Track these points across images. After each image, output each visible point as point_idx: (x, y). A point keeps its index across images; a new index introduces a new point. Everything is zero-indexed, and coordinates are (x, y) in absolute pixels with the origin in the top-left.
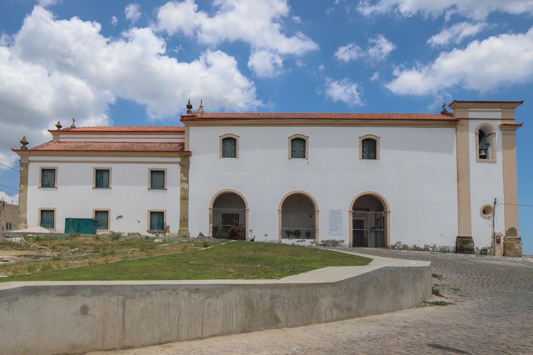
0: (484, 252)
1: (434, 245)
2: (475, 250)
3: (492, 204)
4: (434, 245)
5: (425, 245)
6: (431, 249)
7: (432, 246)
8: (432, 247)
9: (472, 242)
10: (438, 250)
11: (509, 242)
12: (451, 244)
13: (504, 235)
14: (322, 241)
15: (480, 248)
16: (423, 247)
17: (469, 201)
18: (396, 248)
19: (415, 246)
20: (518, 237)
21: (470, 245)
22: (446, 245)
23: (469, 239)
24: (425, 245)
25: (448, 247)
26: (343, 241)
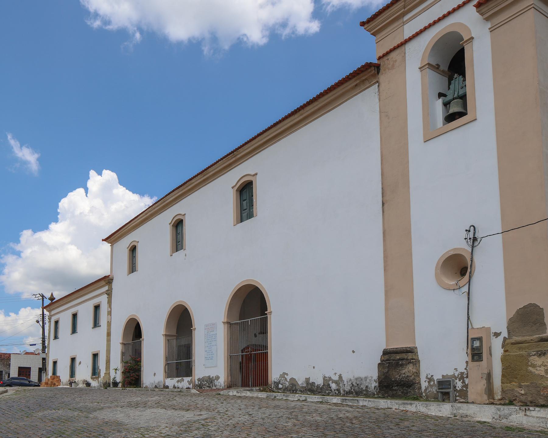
0: (445, 390)
1: (340, 377)
2: (424, 384)
3: (464, 246)
4: (340, 377)
5: (324, 378)
6: (334, 386)
7: (336, 378)
8: (336, 382)
10: (347, 388)
11: (515, 352)
14: (199, 380)
15: (438, 376)
16: (319, 382)
17: (409, 254)
18: (280, 386)
19: (307, 380)
22: (363, 376)
24: (324, 378)
25: (366, 378)
26: (218, 378)
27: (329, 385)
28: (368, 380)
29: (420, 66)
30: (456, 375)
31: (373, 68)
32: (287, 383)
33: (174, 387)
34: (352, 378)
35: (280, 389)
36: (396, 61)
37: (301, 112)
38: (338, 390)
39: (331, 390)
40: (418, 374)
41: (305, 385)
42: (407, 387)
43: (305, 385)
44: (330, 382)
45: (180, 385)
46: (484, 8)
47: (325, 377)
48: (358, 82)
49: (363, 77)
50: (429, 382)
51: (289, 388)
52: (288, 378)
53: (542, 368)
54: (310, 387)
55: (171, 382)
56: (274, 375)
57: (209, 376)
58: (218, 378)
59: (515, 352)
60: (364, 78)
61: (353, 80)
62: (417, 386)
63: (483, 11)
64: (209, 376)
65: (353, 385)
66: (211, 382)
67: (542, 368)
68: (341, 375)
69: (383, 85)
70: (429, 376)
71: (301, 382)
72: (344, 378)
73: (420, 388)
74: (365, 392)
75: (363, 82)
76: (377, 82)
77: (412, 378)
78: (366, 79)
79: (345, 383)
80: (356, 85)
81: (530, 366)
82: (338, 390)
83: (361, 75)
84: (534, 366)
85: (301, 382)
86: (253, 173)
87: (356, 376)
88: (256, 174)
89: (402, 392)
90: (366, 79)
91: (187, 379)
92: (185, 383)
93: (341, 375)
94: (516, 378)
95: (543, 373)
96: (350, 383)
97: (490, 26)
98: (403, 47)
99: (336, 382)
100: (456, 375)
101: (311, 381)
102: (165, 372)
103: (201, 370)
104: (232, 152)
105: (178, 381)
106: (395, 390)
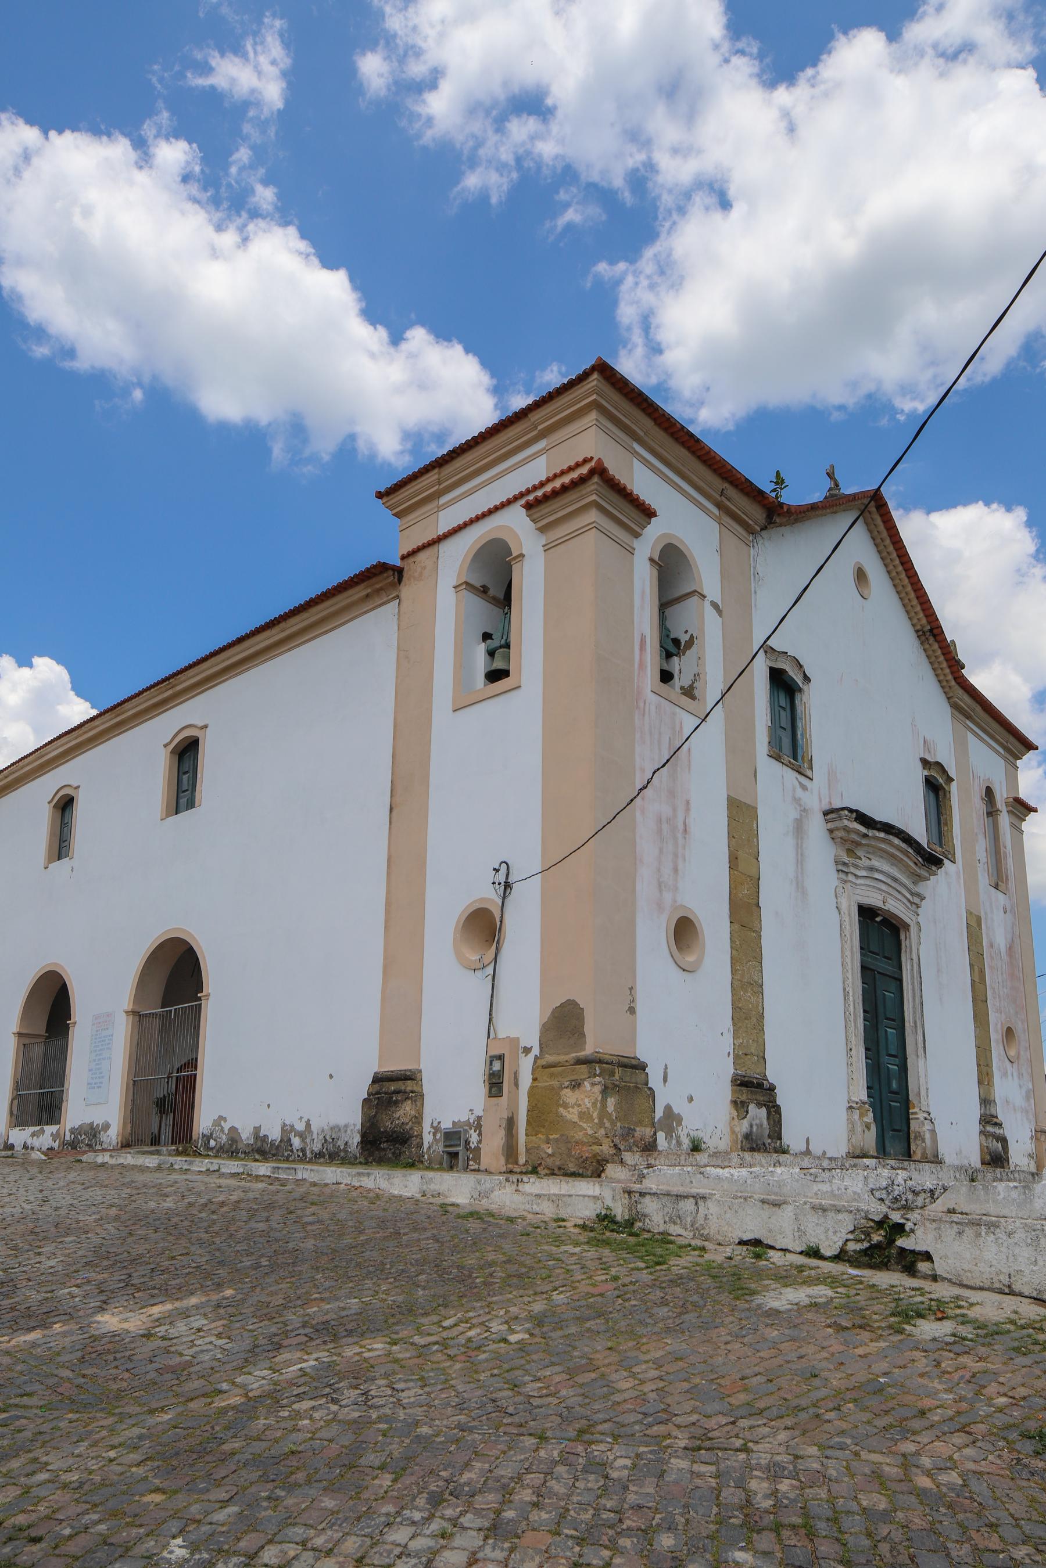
1: (308, 1124)
2: (427, 1138)
4: (308, 1124)
6: (296, 1142)
7: (300, 1127)
8: (301, 1135)
9: (418, 1097)
10: (317, 1147)
12: (342, 1112)
13: (536, 1051)
14: (73, 1131)
15: (447, 1125)
16: (274, 1134)
18: (212, 1143)
20: (588, 1050)
21: (407, 1109)
22: (342, 1122)
23: (400, 1085)
26: (106, 1126)
27: (290, 1140)
28: (349, 1131)
29: (455, 583)
30: (471, 1121)
31: (391, 572)
32: (224, 1137)
33: (25, 1147)
34: (326, 1128)
35: (212, 1149)
36: (424, 568)
37: (283, 625)
38: (303, 1150)
39: (292, 1151)
40: (418, 1119)
41: (252, 1141)
42: (401, 1144)
43: (252, 1141)
44: (292, 1135)
45: (36, 1142)
46: (538, 512)
47: (285, 1125)
48: (369, 590)
49: (377, 583)
50: (434, 1134)
51: (227, 1146)
52: (226, 1127)
53: (575, 1110)
54: (259, 1144)
55: (19, 1136)
56: (203, 1121)
57: (92, 1123)
58: (106, 1126)
59: (544, 1083)
60: (377, 586)
61: (362, 586)
62: (415, 1142)
63: (535, 516)
64: (92, 1123)
65: (326, 1140)
66: (95, 1136)
67: (575, 1110)
68: (309, 1120)
69: (404, 604)
70: (435, 1124)
71: (246, 1135)
72: (314, 1128)
73: (420, 1145)
74: (342, 1154)
75: (378, 591)
76: (398, 597)
77: (408, 1127)
78: (381, 589)
79: (315, 1136)
80: (367, 596)
81: (561, 1106)
82: (303, 1150)
83: (374, 580)
84: (566, 1106)
85: (246, 1135)
86: (200, 724)
87: (332, 1124)
88: (206, 727)
89: (393, 1153)
90: (381, 589)
91: (50, 1129)
92: (46, 1137)
93: (309, 1120)
94: (544, 1127)
95: (575, 1119)
96: (321, 1137)
97: (544, 543)
98: (435, 547)
99: (301, 1135)
100: (471, 1121)
101: (262, 1133)
102: (11, 1114)
103: (76, 1113)
104: (167, 679)
105: (33, 1135)
106: (384, 1149)
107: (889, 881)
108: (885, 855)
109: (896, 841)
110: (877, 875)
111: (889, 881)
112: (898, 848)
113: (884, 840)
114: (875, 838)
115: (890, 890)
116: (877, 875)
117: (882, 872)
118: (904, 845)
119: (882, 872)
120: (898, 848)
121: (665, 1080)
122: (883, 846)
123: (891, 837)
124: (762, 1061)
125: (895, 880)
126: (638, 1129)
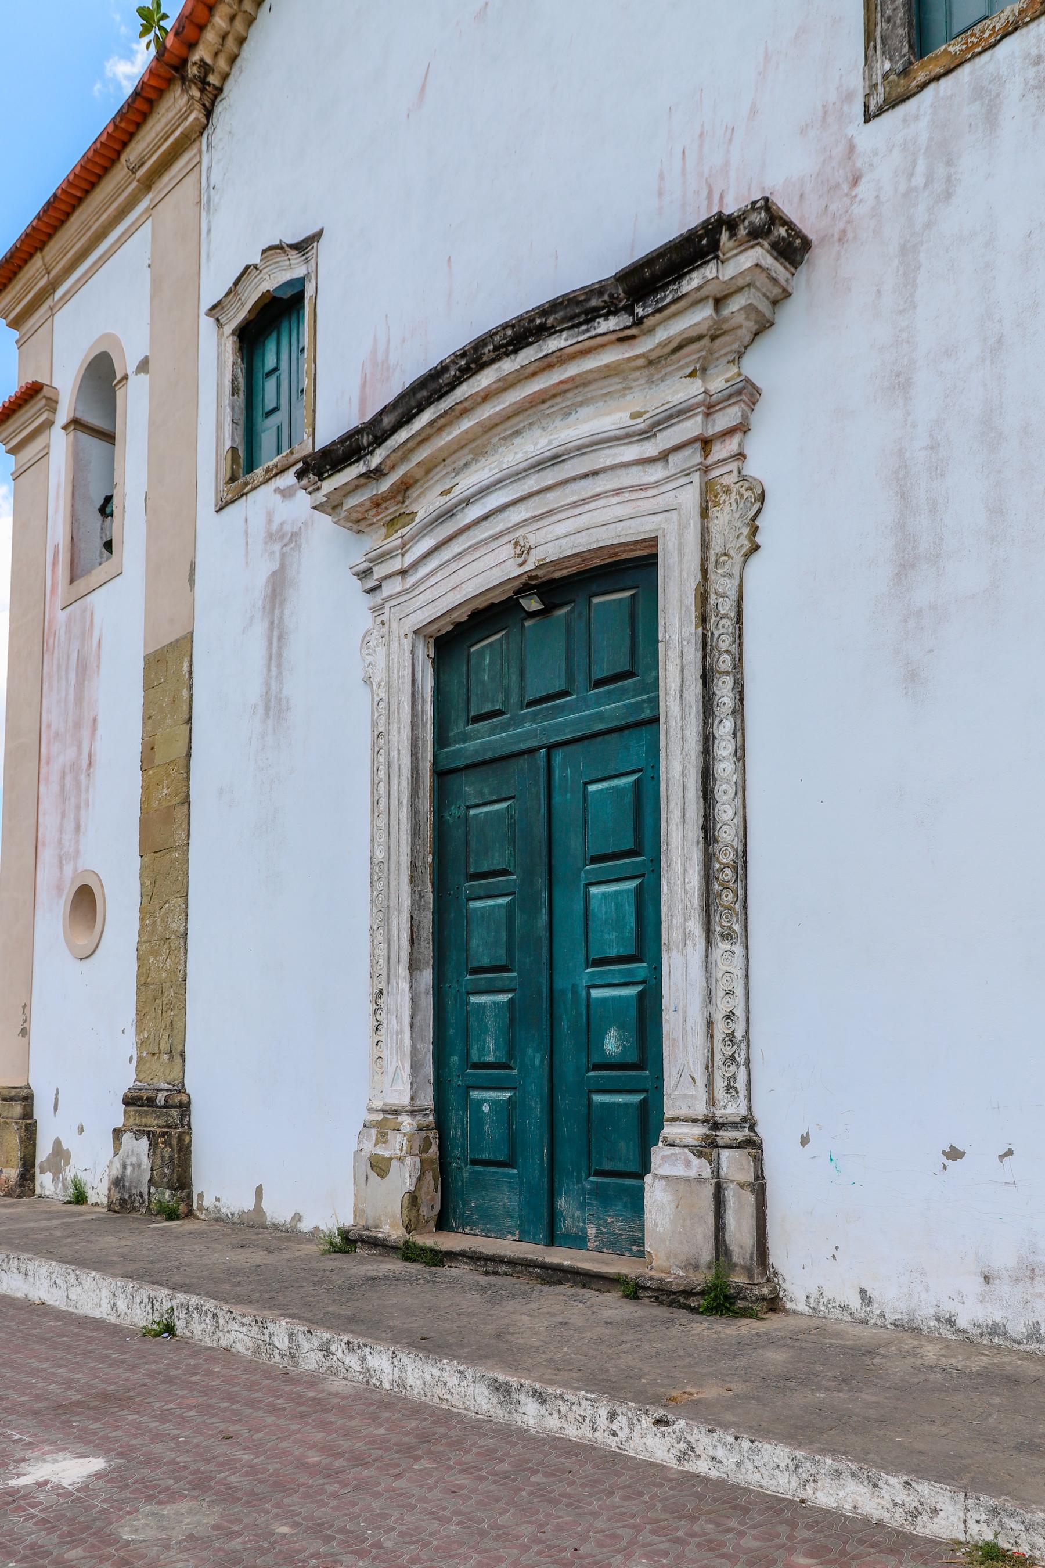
107: (532, 483)
108: (519, 422)
109: (485, 379)
110: (474, 512)
111: (532, 483)
112: (507, 384)
113: (463, 410)
114: (422, 439)
115: (552, 499)
116: (474, 512)
117: (484, 491)
118: (528, 355)
119: (484, 491)
120: (507, 384)
121: (56, 1109)
122: (466, 424)
123: (463, 391)
124: (178, 1059)
125: (556, 459)
126: (4, 1170)
